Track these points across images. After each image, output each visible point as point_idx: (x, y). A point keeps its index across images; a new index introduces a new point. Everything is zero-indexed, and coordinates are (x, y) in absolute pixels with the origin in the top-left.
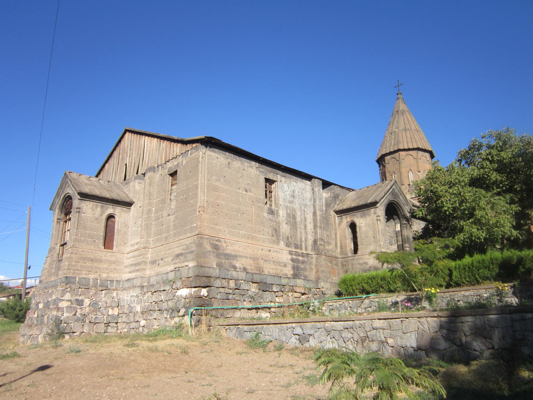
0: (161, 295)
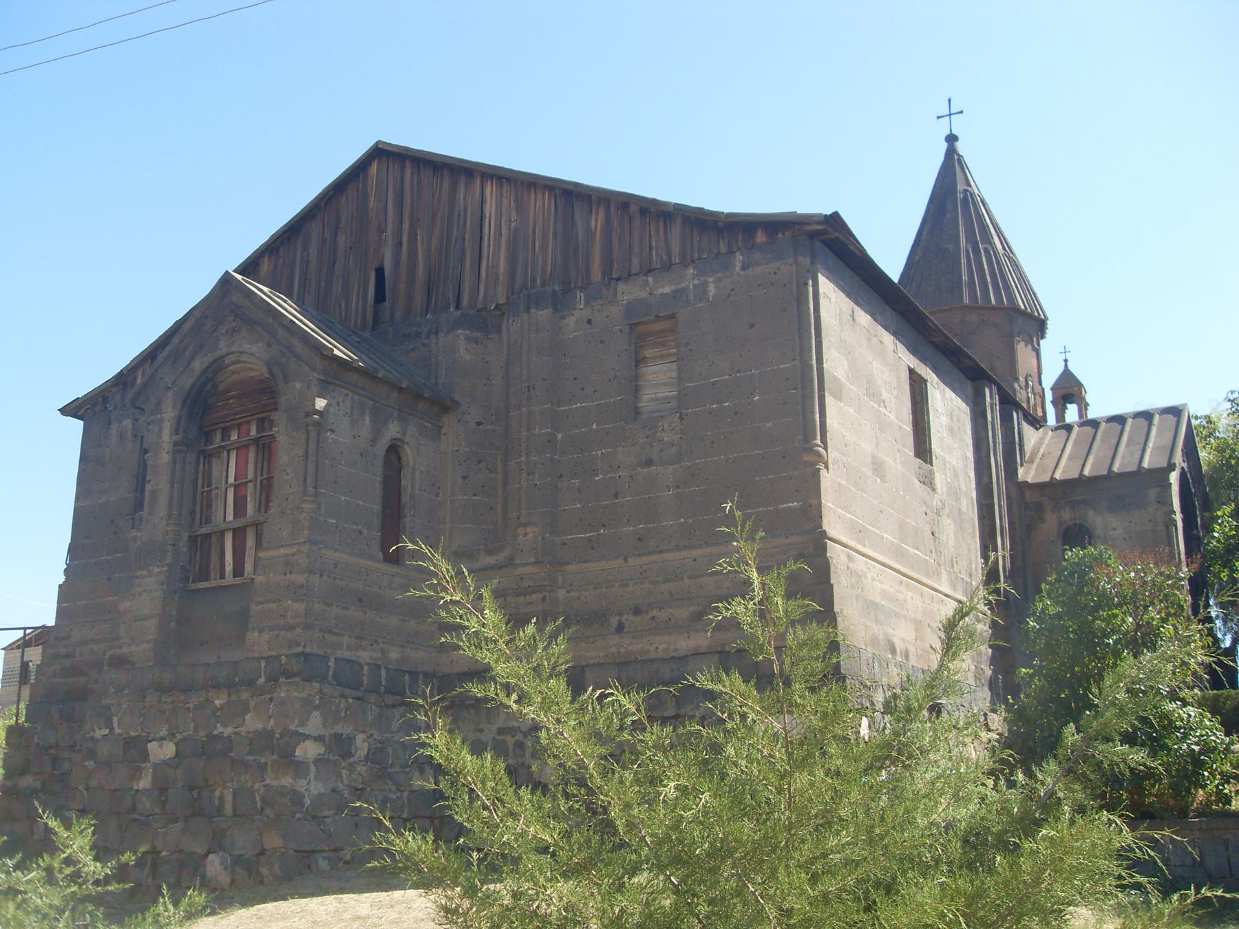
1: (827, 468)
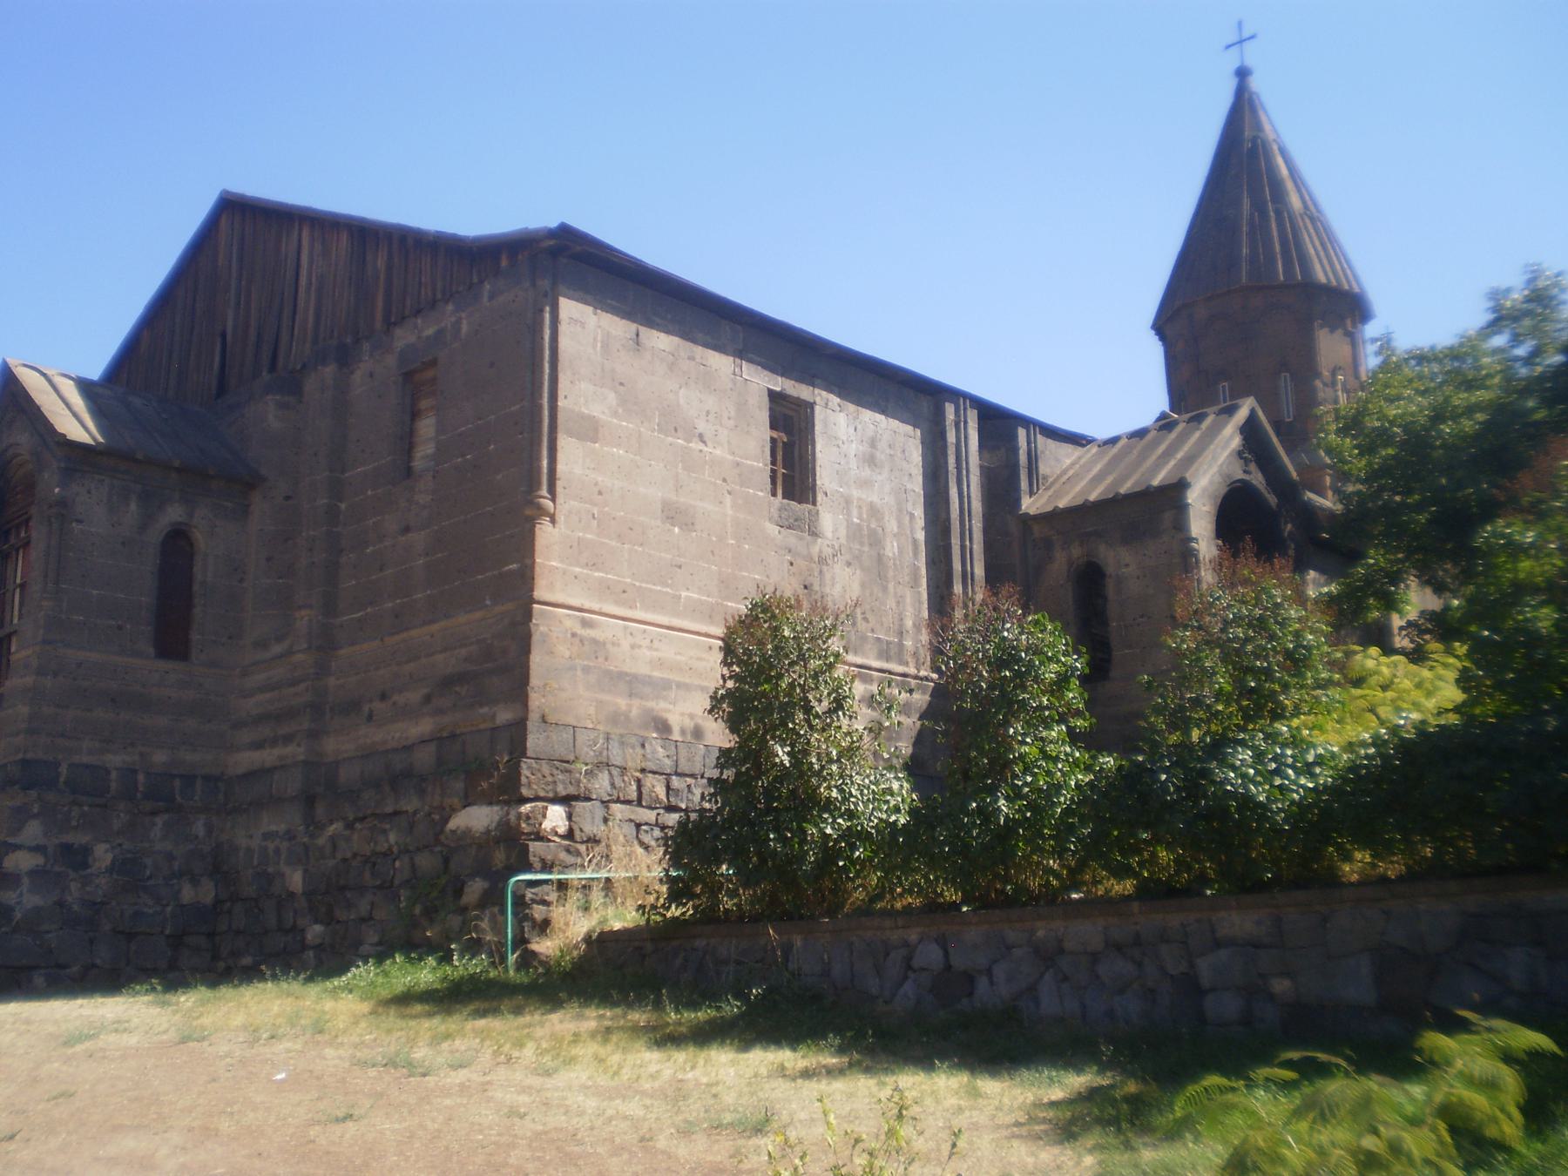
0: (384, 832)
1: (553, 521)
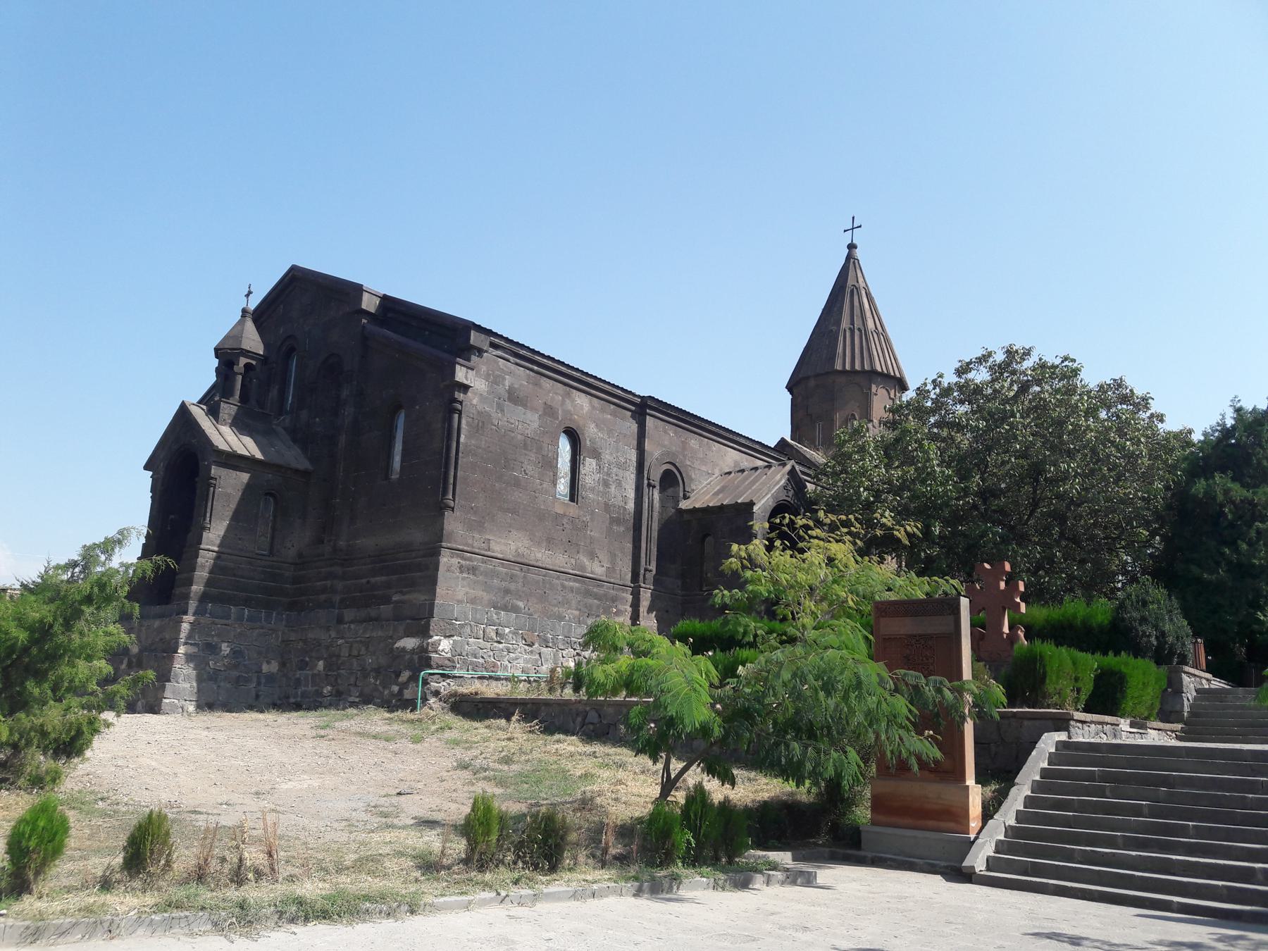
1: (453, 509)
